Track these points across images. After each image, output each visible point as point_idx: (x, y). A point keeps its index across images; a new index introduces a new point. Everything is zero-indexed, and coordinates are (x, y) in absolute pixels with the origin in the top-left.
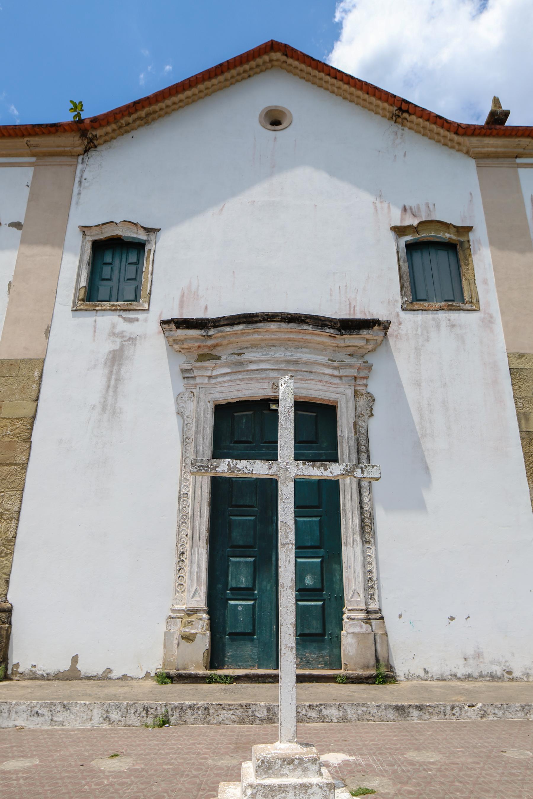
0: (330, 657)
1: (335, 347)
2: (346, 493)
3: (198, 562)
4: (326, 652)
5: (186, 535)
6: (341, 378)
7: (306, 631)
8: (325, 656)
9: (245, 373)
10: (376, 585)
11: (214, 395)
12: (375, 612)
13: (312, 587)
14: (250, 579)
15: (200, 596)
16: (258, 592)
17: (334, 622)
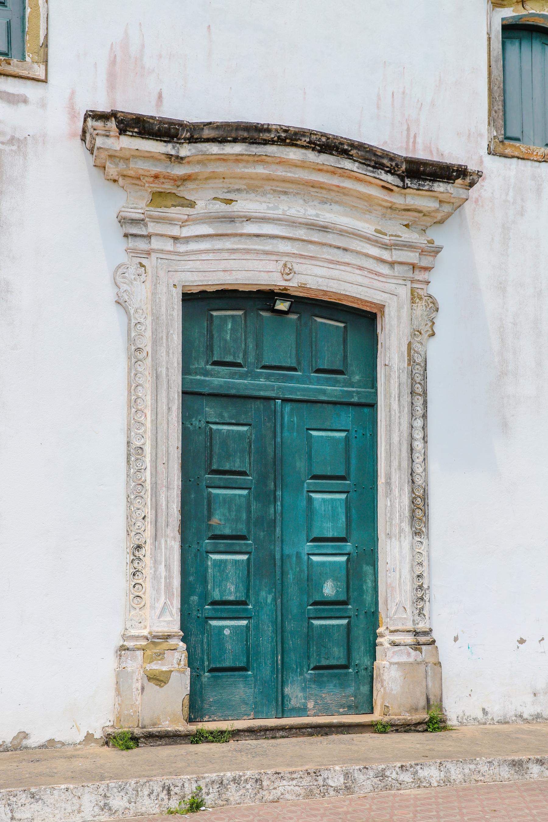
0: (355, 697)
1: (387, 208)
2: (392, 458)
3: (166, 561)
4: (351, 690)
5: (144, 518)
6: (392, 264)
7: (324, 663)
8: (349, 696)
9: (236, 239)
10: (427, 596)
11: (183, 273)
13: (333, 599)
14: (241, 587)
15: (172, 615)
16: (254, 606)
17: (362, 648)
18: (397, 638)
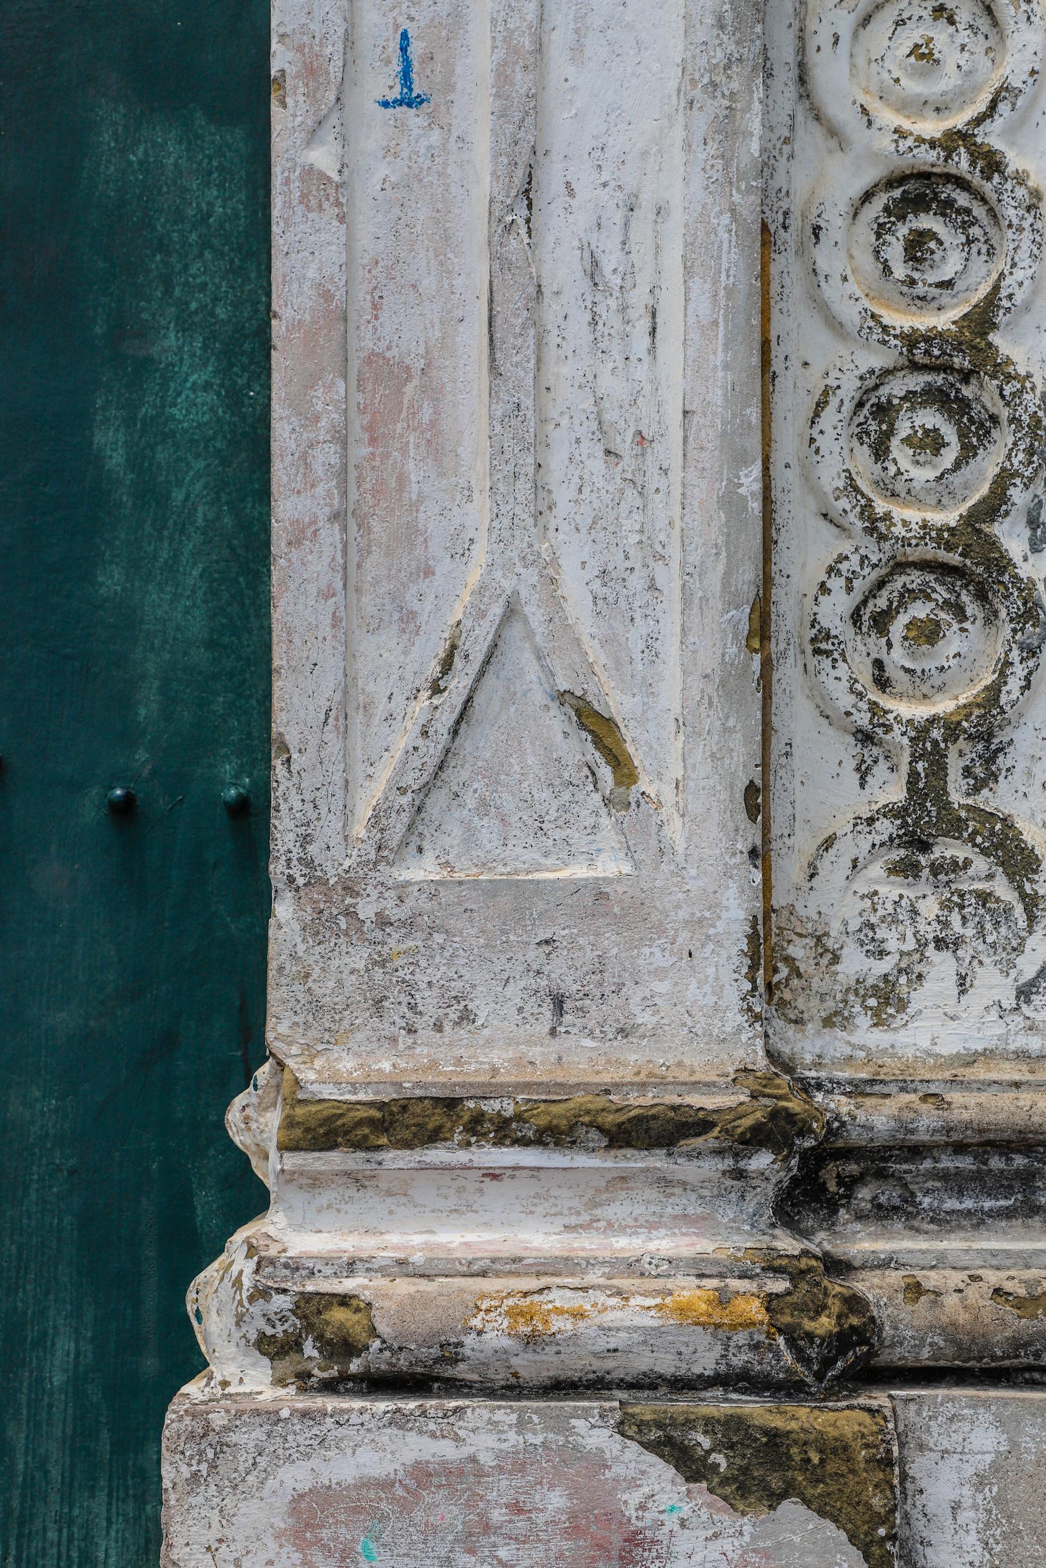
18: (408, 1238)
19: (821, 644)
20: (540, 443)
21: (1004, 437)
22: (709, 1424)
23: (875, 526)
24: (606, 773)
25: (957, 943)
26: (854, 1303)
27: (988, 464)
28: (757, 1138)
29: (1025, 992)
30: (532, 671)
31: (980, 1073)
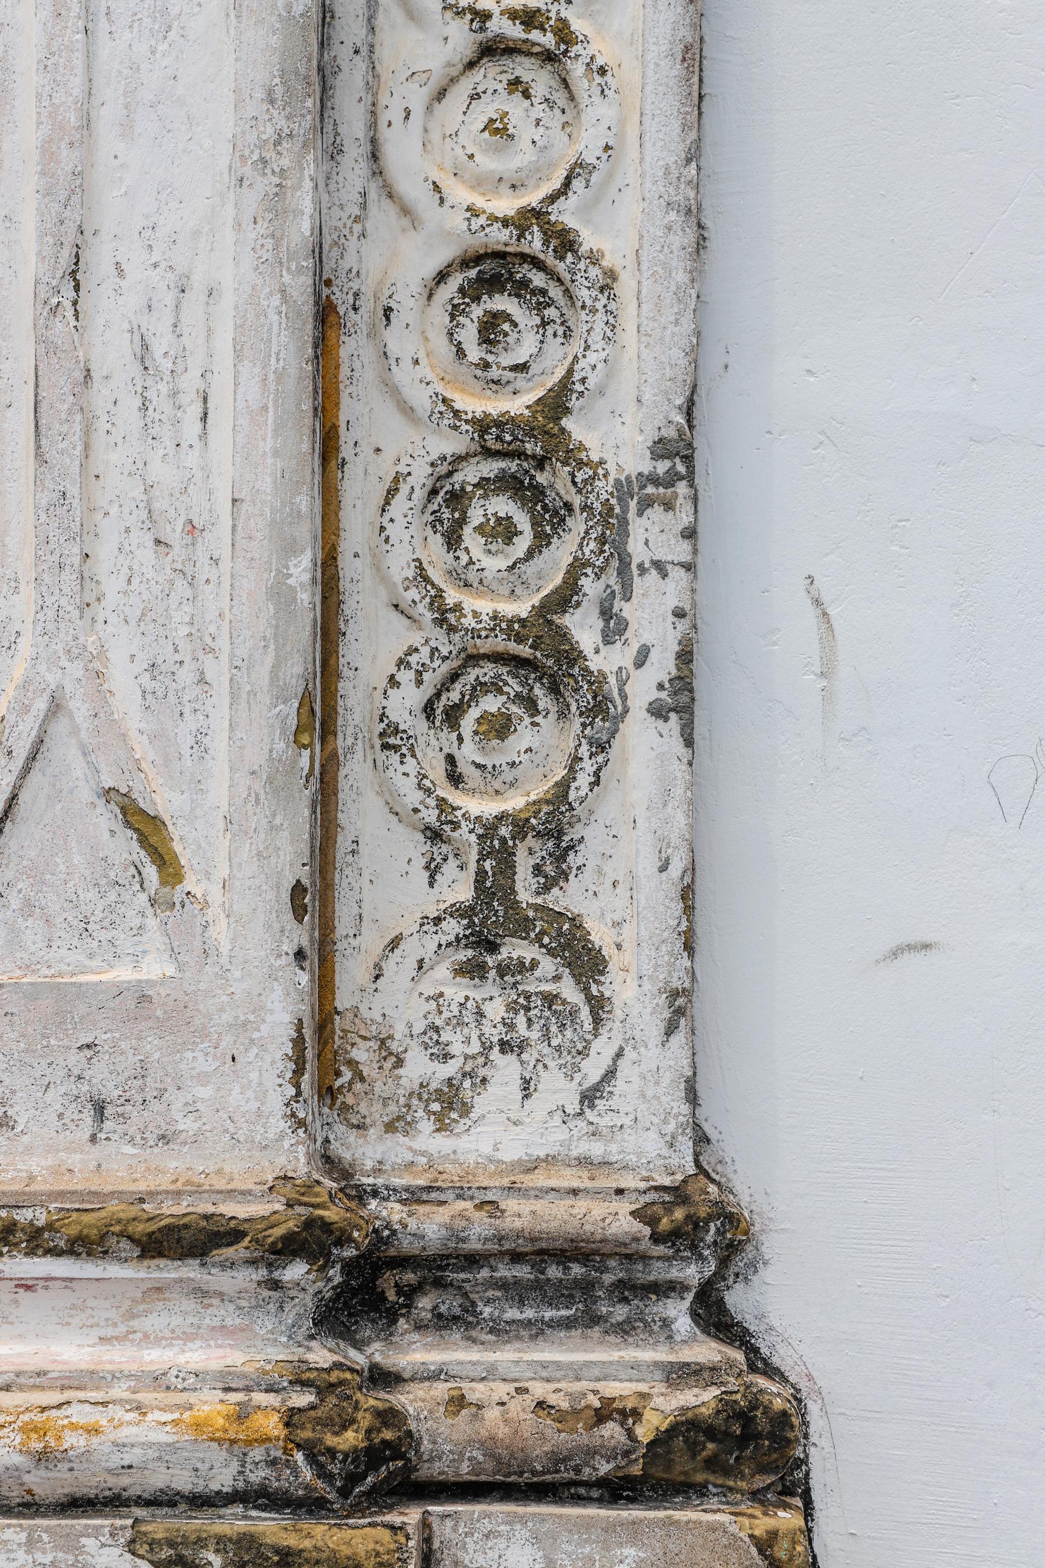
10: (651, 613)
12: (572, 1279)
19: (391, 739)
20: (84, 531)
21: (577, 524)
22: (221, 1543)
23: (444, 616)
24: (151, 872)
25: (522, 1046)
26: (389, 1416)
27: (561, 553)
28: (289, 1248)
29: (589, 1097)
30: (79, 768)
31: (540, 1179)
